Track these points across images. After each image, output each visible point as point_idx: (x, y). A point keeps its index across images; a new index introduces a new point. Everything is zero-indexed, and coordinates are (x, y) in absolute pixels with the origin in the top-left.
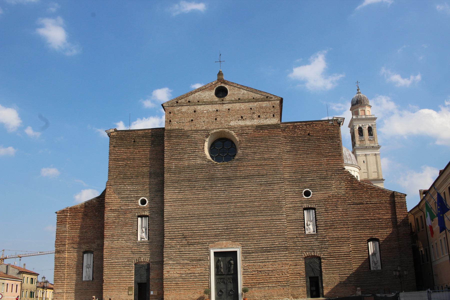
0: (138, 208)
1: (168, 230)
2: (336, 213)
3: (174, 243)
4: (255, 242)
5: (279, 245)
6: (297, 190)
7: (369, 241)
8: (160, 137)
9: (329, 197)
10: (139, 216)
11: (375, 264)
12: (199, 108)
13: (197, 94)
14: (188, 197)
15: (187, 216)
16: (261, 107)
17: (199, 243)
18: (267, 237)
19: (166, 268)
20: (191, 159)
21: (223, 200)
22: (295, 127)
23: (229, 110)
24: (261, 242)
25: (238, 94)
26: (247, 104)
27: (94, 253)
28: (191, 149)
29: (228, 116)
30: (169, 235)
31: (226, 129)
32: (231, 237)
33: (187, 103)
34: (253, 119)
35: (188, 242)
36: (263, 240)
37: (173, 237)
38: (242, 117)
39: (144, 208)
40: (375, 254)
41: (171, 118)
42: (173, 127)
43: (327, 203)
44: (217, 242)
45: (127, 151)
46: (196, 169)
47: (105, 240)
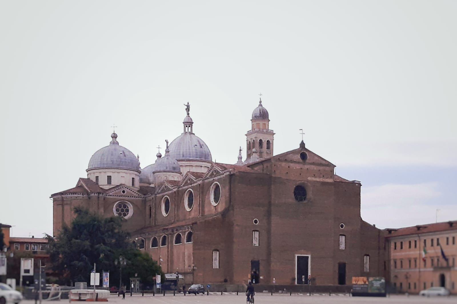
12: (292, 165)
16: (324, 170)
19: (272, 264)
27: (220, 252)
34: (320, 177)
38: (314, 175)
39: (256, 225)
42: (277, 176)
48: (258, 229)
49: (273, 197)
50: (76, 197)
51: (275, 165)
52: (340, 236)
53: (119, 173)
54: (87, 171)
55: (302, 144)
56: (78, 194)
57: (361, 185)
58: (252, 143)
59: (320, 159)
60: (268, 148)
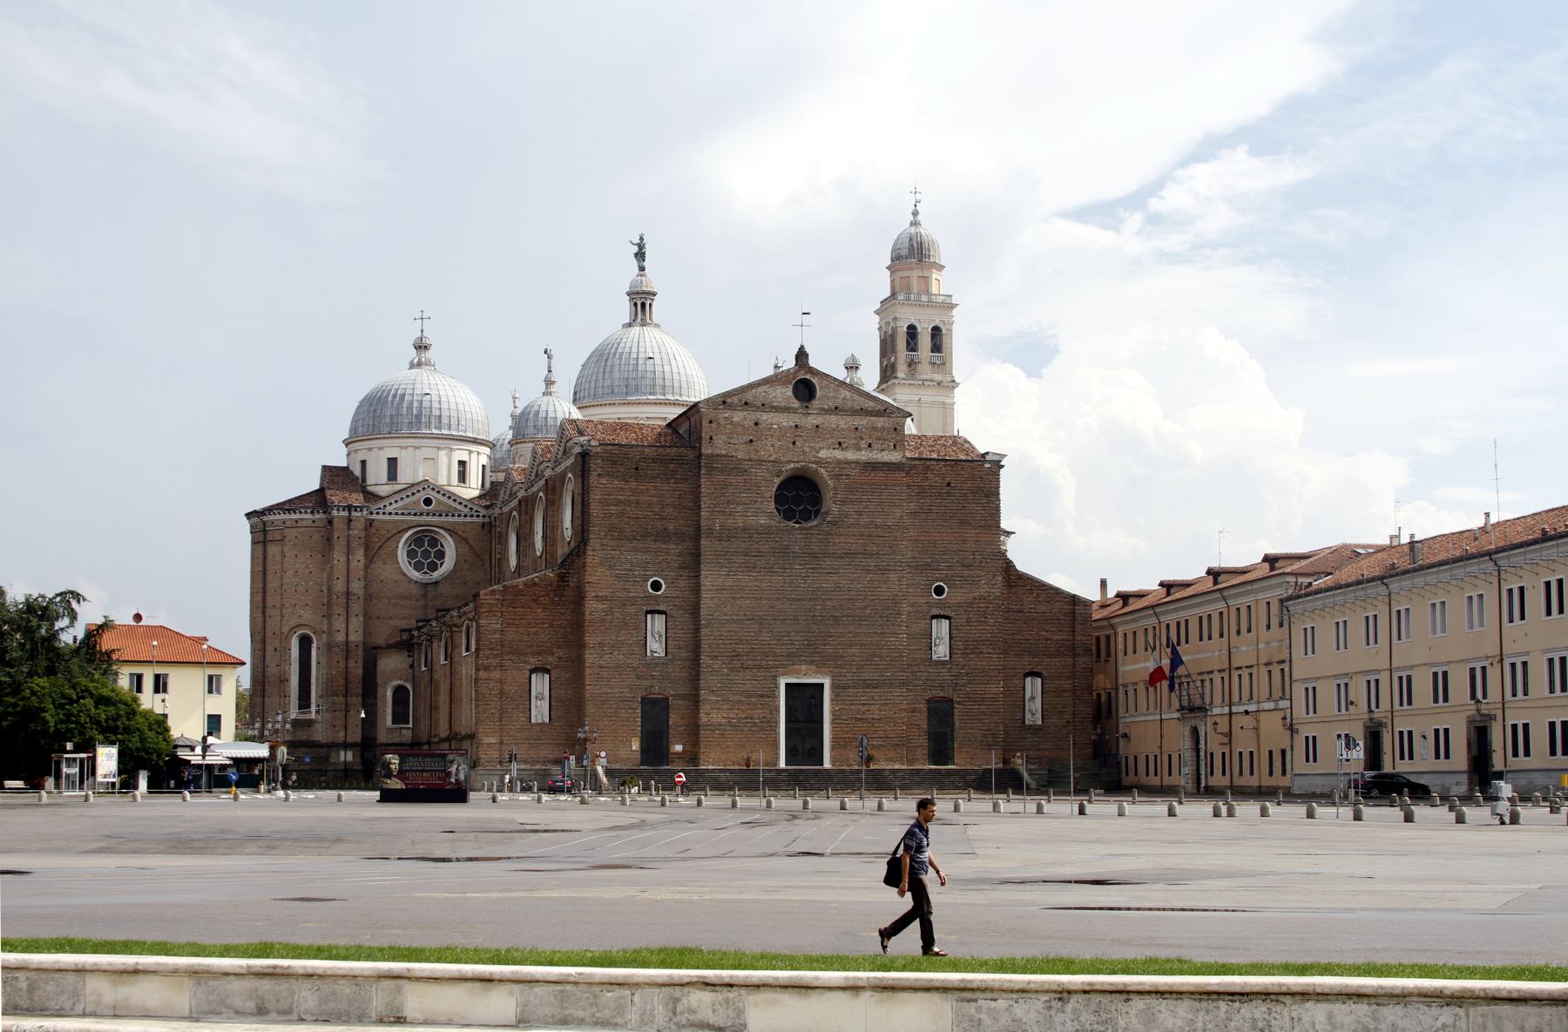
0: (646, 597)
1: (708, 642)
2: (984, 627)
3: (717, 664)
4: (855, 670)
5: (892, 678)
6: (923, 583)
7: (1027, 675)
8: (687, 464)
9: (974, 599)
10: (648, 612)
11: (1033, 715)
12: (764, 417)
13: (761, 389)
14: (744, 584)
15: (741, 618)
16: (875, 429)
17: (760, 667)
18: (874, 663)
19: (705, 708)
20: (749, 514)
21: (803, 593)
22: (928, 467)
23: (817, 427)
24: (865, 671)
25: (835, 397)
26: (849, 419)
27: (552, 672)
28: (750, 495)
29: (817, 439)
30: (709, 650)
31: (813, 463)
32: (814, 659)
33: (742, 405)
35: (742, 664)
36: (866, 667)
37: (716, 654)
38: (840, 444)
39: (659, 595)
40: (1034, 698)
41: (712, 432)
43: (970, 609)
44: (791, 667)
45: (624, 486)
46: (758, 533)
47: (587, 652)
48: (662, 607)
49: (704, 514)
50: (297, 522)
51: (711, 422)
52: (934, 621)
53: (419, 448)
54: (347, 443)
55: (802, 355)
56: (300, 512)
57: (1003, 466)
58: (891, 336)
59: (856, 397)
60: (937, 347)
